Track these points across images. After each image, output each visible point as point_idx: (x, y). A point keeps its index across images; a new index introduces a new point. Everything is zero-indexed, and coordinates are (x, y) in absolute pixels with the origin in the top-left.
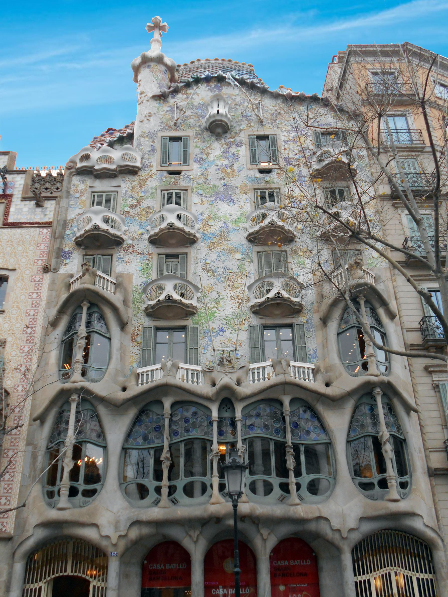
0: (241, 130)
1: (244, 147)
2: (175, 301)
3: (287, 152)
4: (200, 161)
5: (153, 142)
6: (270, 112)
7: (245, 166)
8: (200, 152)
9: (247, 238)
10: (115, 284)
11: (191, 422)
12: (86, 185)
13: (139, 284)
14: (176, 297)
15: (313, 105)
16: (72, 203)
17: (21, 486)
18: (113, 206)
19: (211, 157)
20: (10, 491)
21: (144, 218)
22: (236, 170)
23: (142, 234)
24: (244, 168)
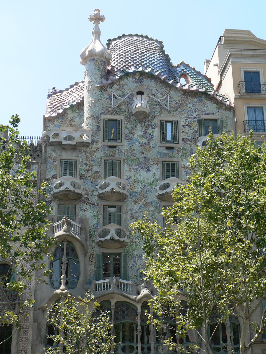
0: (155, 116)
1: (157, 129)
2: (115, 241)
3: (184, 134)
4: (128, 139)
5: (98, 123)
6: (174, 102)
7: (157, 144)
8: (128, 132)
9: (157, 196)
10: (80, 228)
11: (125, 313)
12: (57, 154)
13: (93, 225)
14: (116, 238)
15: (203, 97)
16: (48, 167)
17: (32, 345)
18: (75, 170)
19: (136, 136)
20: (26, 348)
21: (94, 179)
22: (152, 146)
23: (93, 191)
24: (156, 145)
